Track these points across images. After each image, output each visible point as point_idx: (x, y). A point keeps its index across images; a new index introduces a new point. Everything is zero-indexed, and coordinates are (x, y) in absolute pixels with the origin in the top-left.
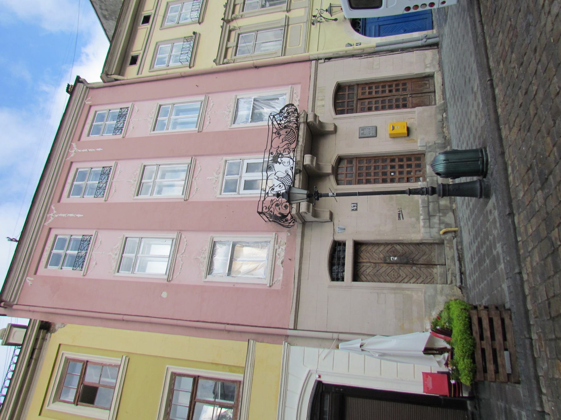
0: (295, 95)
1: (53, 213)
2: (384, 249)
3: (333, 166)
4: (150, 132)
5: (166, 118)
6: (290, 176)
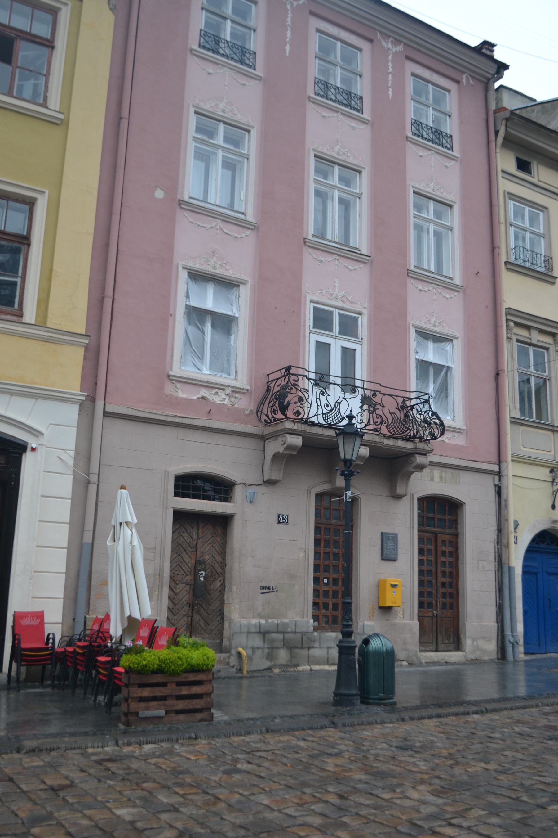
2: (217, 561)
4: (413, 187)
5: (431, 216)
6: (340, 422)
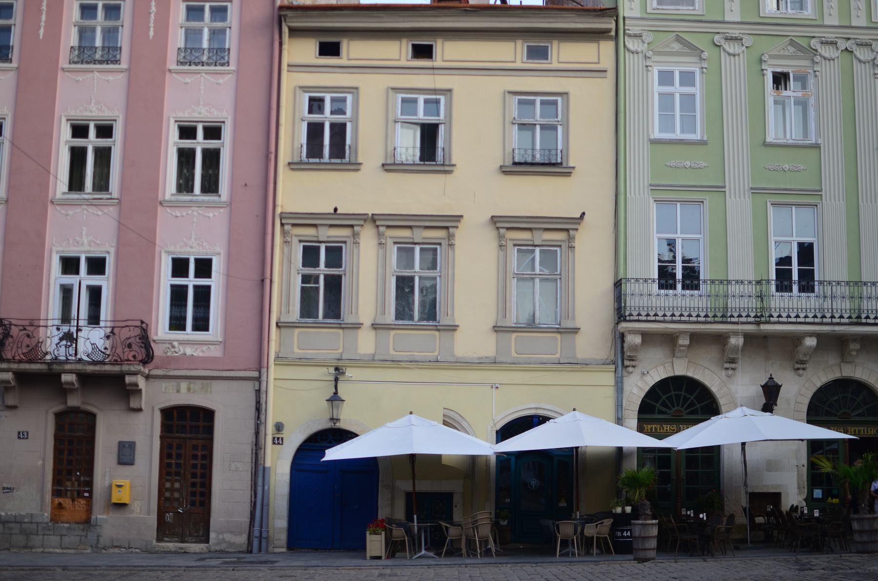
0: (205, 348)
3: (79, 408)
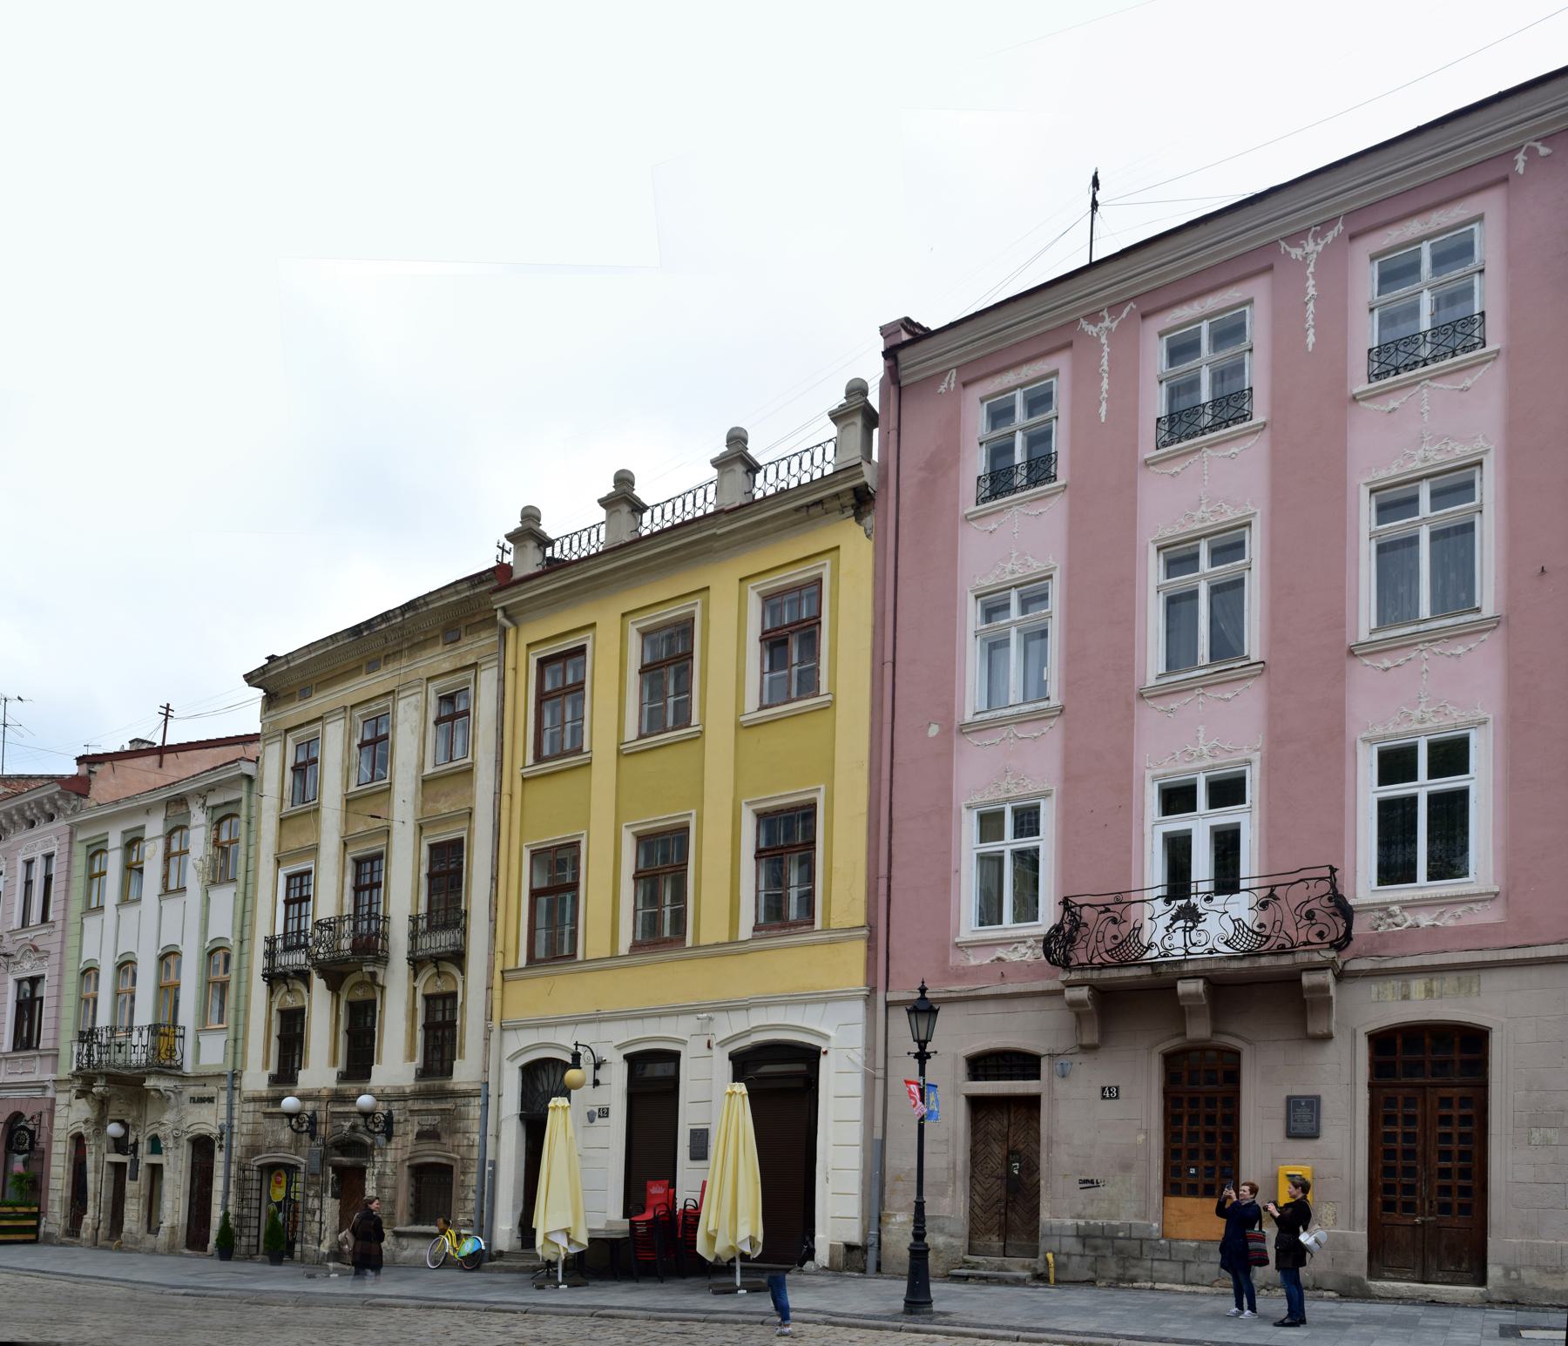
1: (1112, 322)
